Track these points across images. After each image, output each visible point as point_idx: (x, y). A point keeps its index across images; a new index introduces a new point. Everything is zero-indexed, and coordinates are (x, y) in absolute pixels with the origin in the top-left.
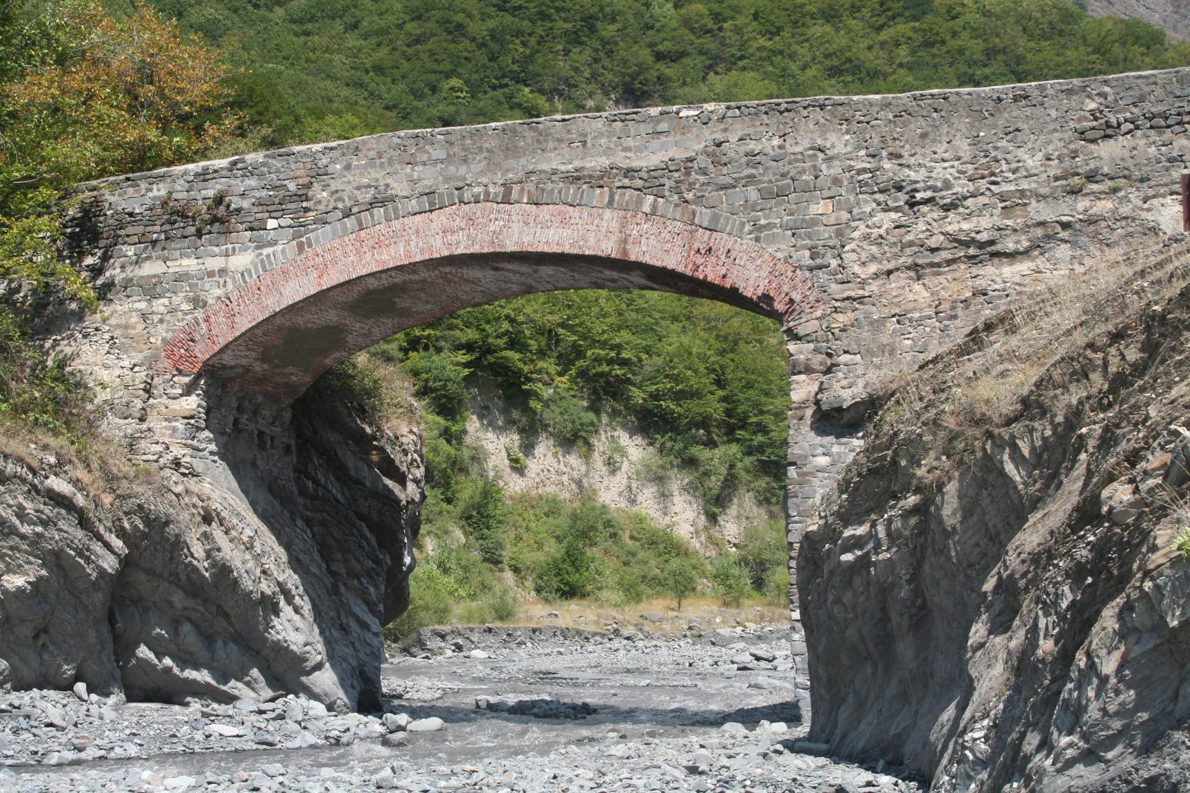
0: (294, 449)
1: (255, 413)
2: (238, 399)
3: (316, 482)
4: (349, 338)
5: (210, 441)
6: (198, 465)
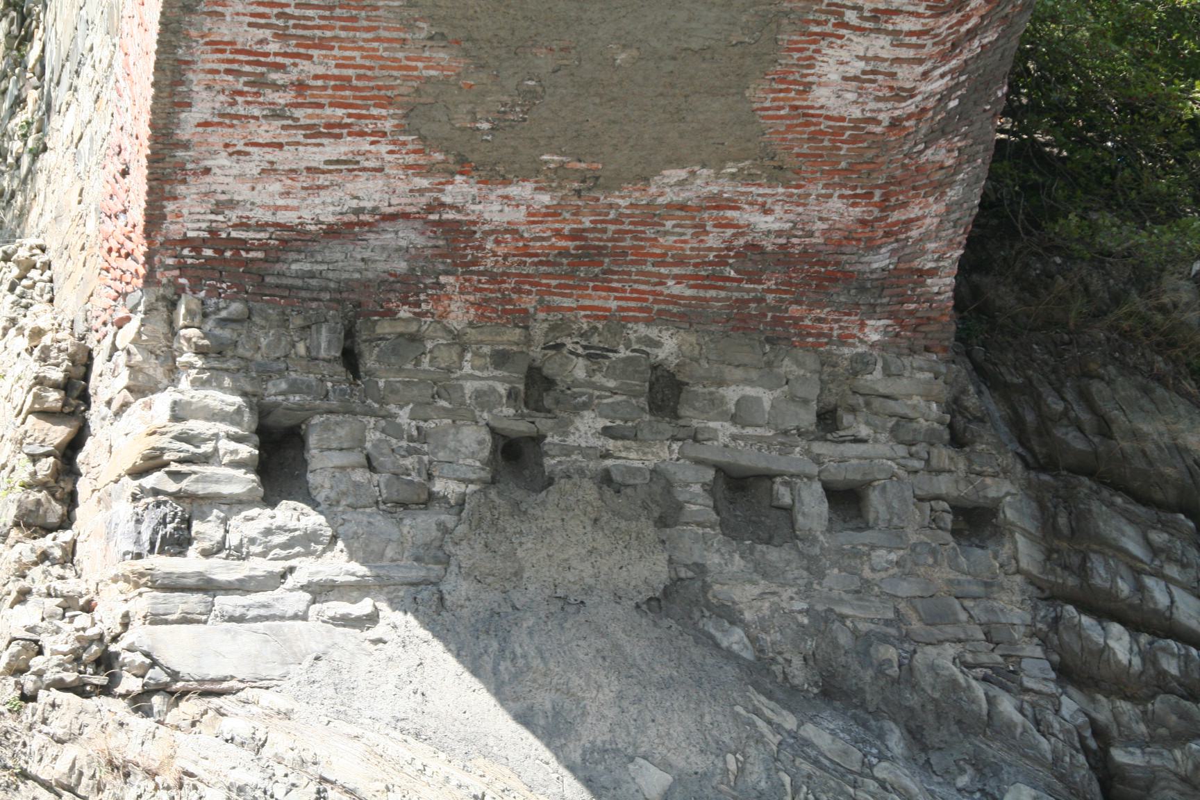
0: (1015, 509)
1: (665, 393)
2: (501, 359)
5: (306, 542)
6: (186, 649)
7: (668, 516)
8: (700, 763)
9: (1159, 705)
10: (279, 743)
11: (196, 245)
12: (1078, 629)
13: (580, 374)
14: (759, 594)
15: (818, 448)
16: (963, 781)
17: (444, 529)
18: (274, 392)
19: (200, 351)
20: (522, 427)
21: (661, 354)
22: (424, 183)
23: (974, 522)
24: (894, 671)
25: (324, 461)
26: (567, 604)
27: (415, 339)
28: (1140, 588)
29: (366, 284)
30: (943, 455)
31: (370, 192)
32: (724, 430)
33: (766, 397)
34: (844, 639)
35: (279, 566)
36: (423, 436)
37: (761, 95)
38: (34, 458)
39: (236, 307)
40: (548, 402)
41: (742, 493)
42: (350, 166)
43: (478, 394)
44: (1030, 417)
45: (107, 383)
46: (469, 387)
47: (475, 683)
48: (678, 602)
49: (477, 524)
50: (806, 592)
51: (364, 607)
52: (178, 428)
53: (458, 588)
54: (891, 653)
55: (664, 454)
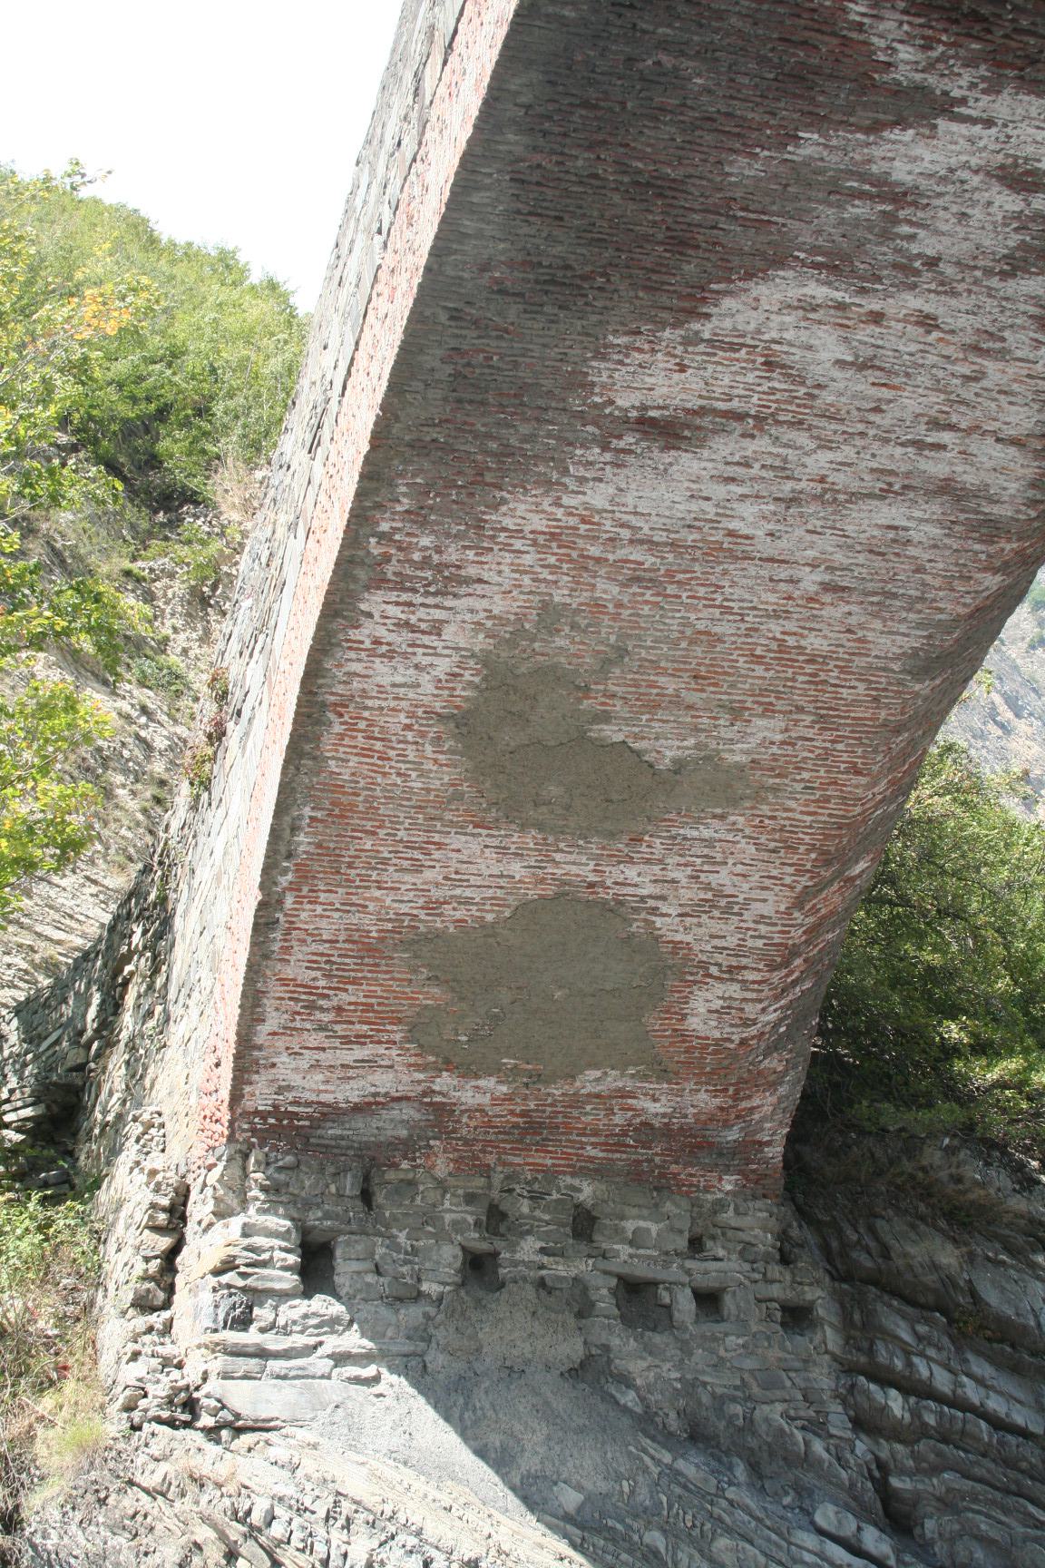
0: (825, 1309)
1: (584, 1224)
2: (470, 1198)
3: (915, 1389)
4: (668, 925)
5: (332, 1324)
6: (245, 1398)
7: (584, 1310)
8: (603, 1486)
9: (922, 1446)
10: (309, 1465)
11: (263, 1116)
12: (867, 1393)
13: (525, 1210)
14: (647, 1367)
15: (689, 1264)
16: (787, 1500)
17: (427, 1316)
18: (313, 1218)
19: (264, 1189)
20: (484, 1246)
21: (582, 1197)
22: (421, 1076)
23: (796, 1317)
24: (740, 1422)
25: (346, 1268)
26: (512, 1372)
27: (412, 1183)
28: (910, 1364)
29: (379, 1145)
30: (775, 1270)
31: (384, 1082)
32: (624, 1250)
33: (654, 1228)
34: (705, 1399)
35: (312, 1341)
36: (415, 1251)
37: (653, 1022)
38: (147, 1260)
39: (289, 1159)
40: (502, 1229)
41: (636, 1294)
42: (370, 1064)
43: (454, 1223)
44: (835, 1244)
45: (199, 1209)
46: (448, 1217)
47: (448, 1428)
48: (591, 1372)
49: (451, 1314)
50: (680, 1366)
51: (370, 1371)
52: (247, 1241)
53: (437, 1360)
54: (737, 1409)
55: (582, 1267)
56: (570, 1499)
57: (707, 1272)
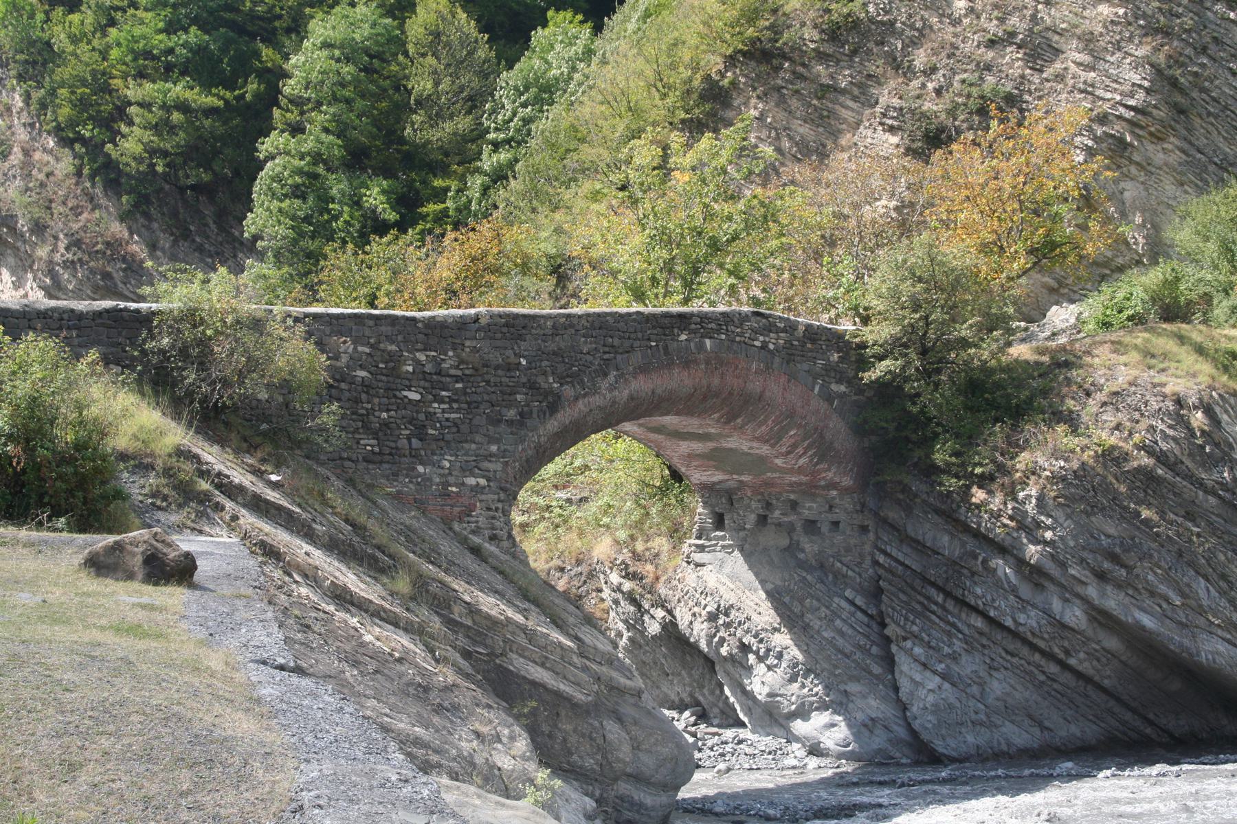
1: (794, 505)
14: (810, 547)
18: (717, 509)
23: (864, 529)
32: (807, 512)
41: (811, 526)
53: (747, 546)
55: (793, 518)
56: (770, 586)
57: (834, 518)
